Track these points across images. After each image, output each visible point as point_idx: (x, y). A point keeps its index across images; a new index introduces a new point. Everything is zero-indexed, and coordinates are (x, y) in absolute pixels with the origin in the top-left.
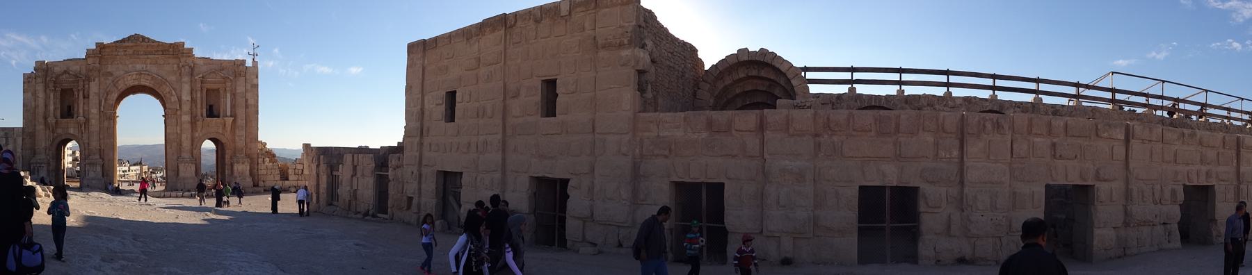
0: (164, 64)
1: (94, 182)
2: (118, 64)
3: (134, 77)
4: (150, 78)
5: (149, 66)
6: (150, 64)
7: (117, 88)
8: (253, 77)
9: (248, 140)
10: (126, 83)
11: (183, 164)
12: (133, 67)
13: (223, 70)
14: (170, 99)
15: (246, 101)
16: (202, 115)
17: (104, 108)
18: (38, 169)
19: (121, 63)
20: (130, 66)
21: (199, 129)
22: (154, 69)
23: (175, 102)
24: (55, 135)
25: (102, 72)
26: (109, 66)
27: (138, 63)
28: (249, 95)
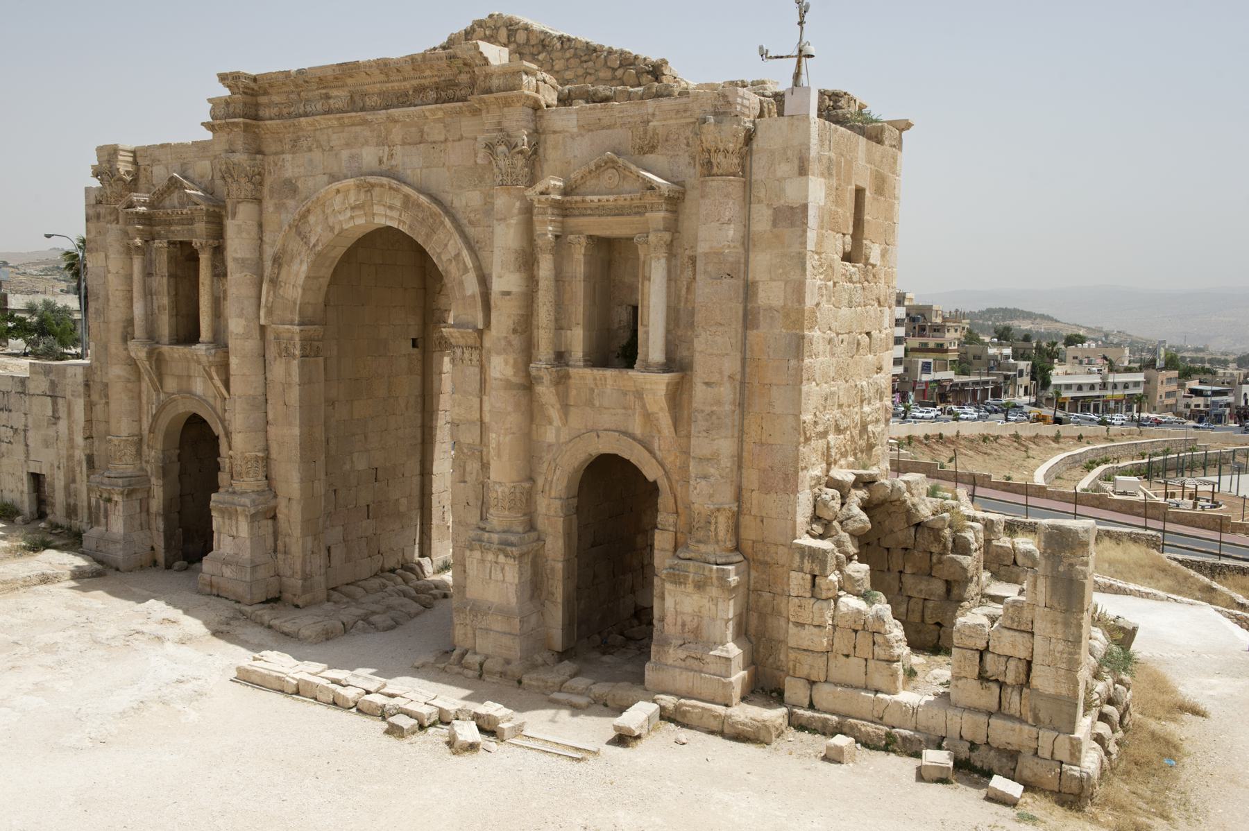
0: (446, 140)
1: (228, 572)
2: (310, 150)
3: (352, 199)
4: (398, 203)
5: (398, 150)
6: (404, 143)
7: (304, 238)
8: (784, 169)
9: (751, 478)
10: (331, 220)
11: (477, 554)
12: (352, 157)
13: (652, 149)
14: (461, 283)
15: (749, 290)
16: (561, 358)
17: (270, 312)
18: (106, 511)
19: (320, 146)
20: (345, 154)
21: (554, 413)
22: (410, 161)
23: (473, 296)
24: (162, 396)
25: (268, 181)
26: (288, 157)
27: (366, 143)
28: (761, 262)
